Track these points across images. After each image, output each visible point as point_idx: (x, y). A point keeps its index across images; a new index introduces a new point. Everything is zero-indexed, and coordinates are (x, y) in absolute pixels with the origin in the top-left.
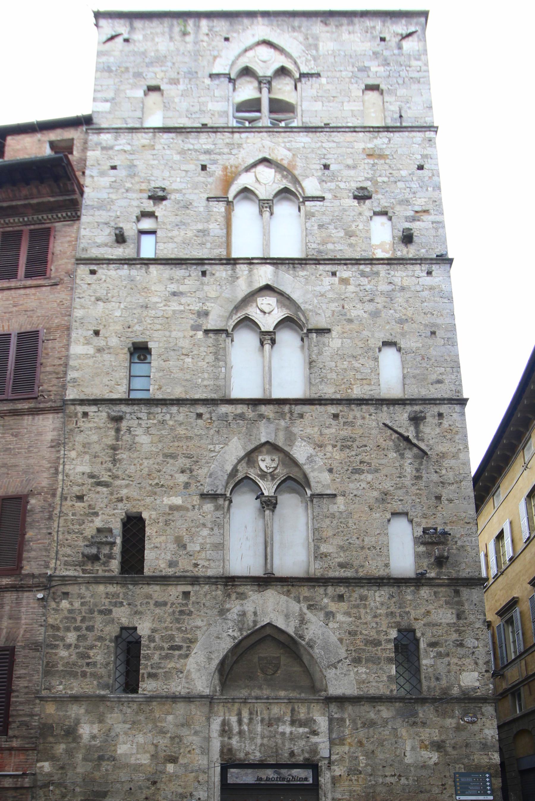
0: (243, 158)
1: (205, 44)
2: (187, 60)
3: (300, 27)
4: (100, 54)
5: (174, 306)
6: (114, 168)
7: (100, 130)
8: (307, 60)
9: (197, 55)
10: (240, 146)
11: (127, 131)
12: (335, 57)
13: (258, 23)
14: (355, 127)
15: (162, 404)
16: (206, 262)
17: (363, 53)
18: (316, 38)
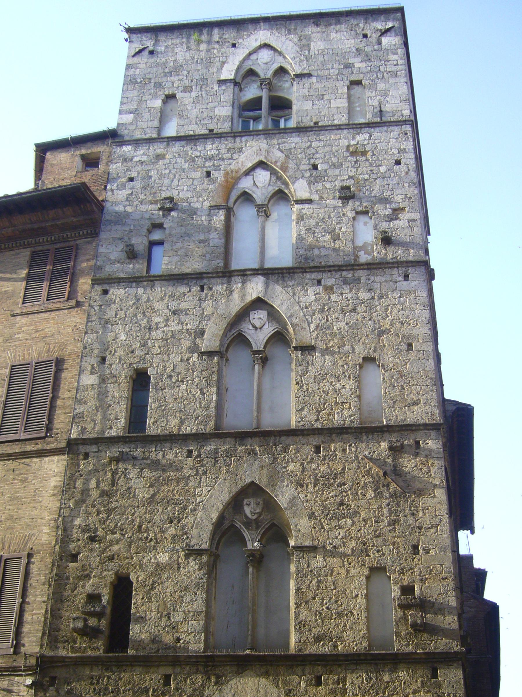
0: (242, 162)
1: (215, 51)
2: (199, 67)
3: (295, 29)
4: (128, 67)
5: (174, 326)
6: (131, 180)
7: (123, 143)
8: (301, 61)
9: (209, 62)
10: (240, 150)
11: (145, 141)
12: (324, 55)
13: (260, 28)
14: (340, 125)
15: (156, 441)
16: (205, 276)
17: (348, 50)
18: (309, 38)
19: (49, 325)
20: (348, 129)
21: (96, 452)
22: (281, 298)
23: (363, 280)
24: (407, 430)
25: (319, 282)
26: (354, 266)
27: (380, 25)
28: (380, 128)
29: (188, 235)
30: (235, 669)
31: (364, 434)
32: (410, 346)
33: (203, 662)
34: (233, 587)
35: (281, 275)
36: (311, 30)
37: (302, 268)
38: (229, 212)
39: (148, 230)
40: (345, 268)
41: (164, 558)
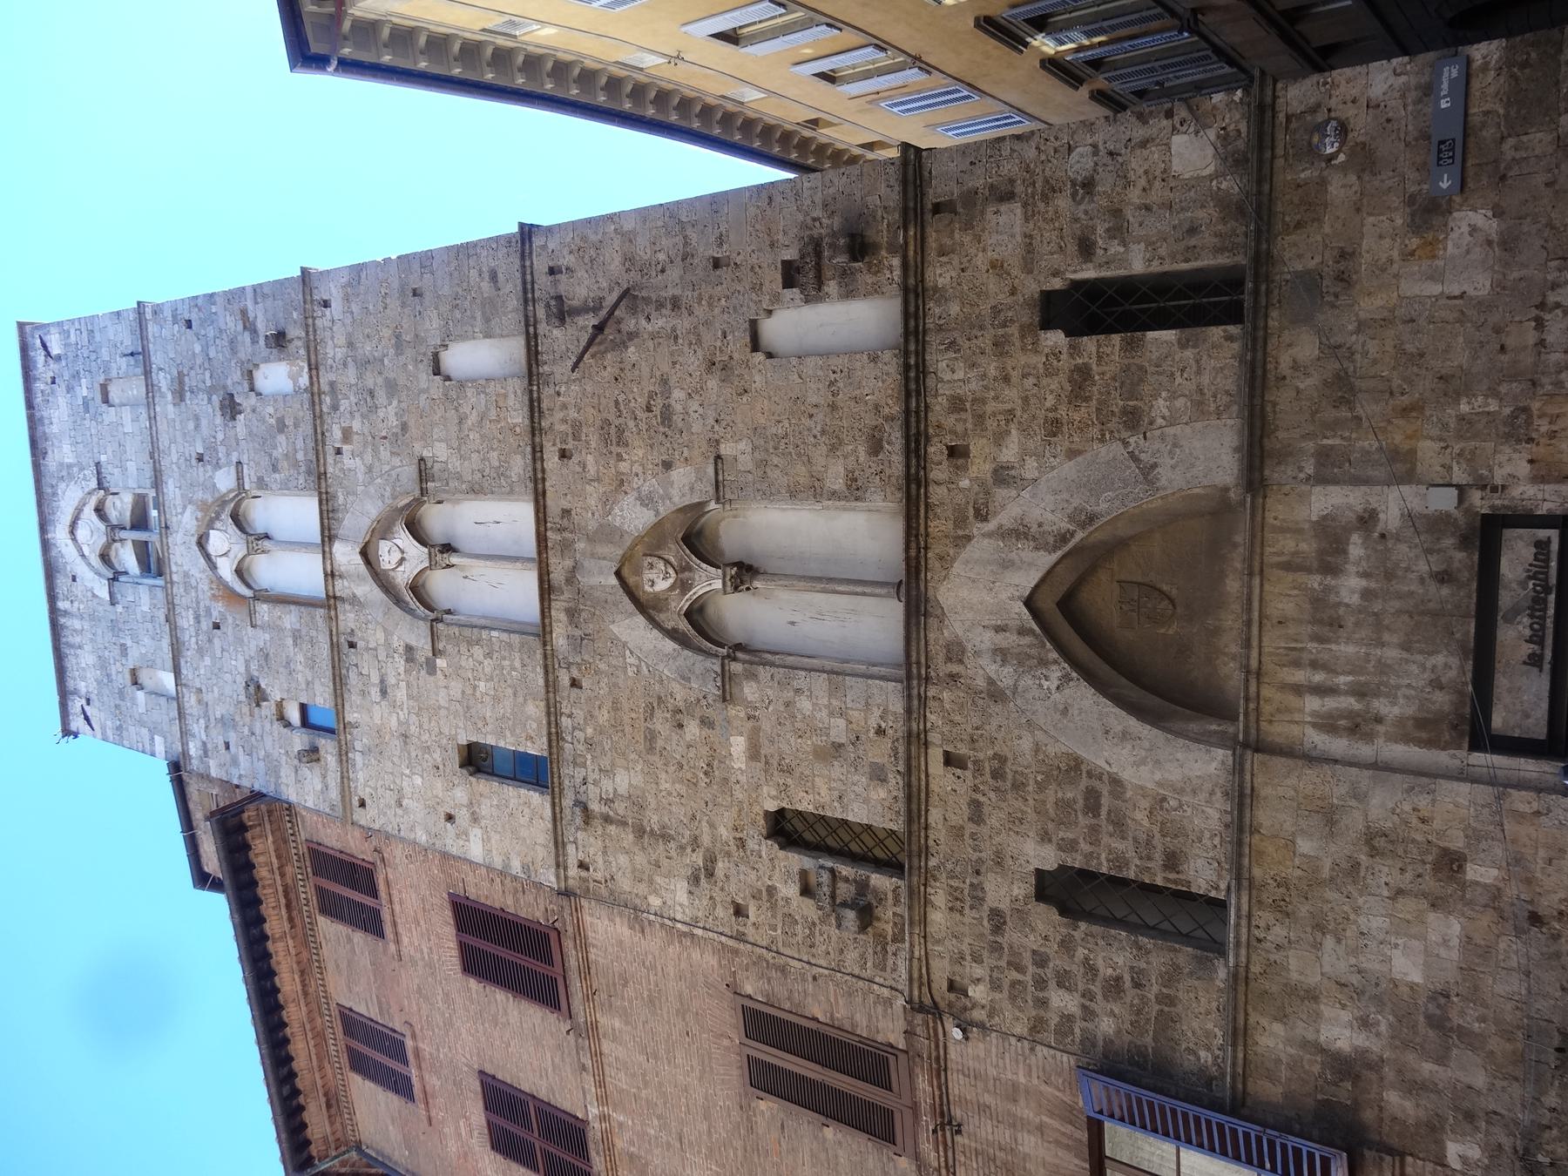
2: (99, 632)
7: (185, 753)
10: (186, 575)
22: (360, 515)
23: (332, 377)
27: (40, 357)
33: (919, 686)
36: (51, 463)
38: (263, 596)
41: (738, 745)
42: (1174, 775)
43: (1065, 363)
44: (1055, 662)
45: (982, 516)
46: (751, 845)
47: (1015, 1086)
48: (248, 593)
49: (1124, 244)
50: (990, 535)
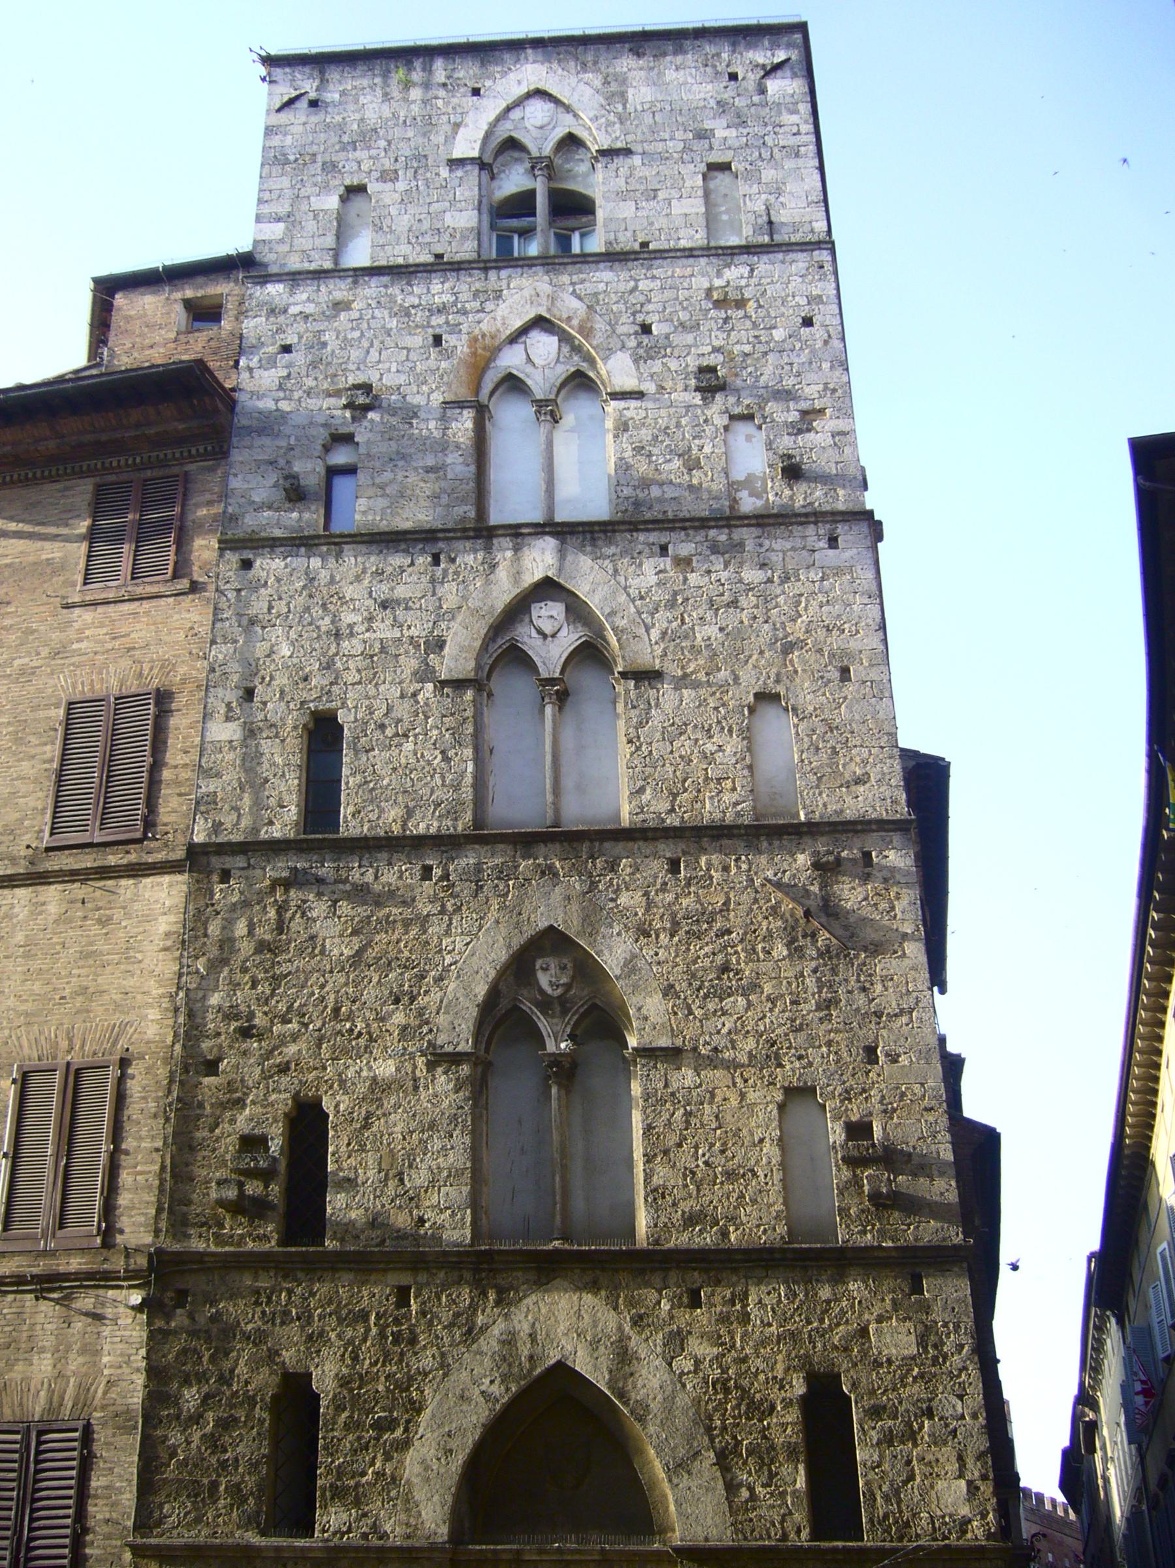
0: (503, 318)
1: (440, 103)
3: (595, 63)
5: (384, 631)
7: (265, 279)
8: (609, 124)
9: (428, 124)
10: (498, 295)
11: (310, 276)
12: (654, 113)
13: (526, 59)
14: (691, 249)
15: (361, 848)
16: (440, 535)
17: (702, 104)
18: (623, 81)
19: (138, 626)
20: (708, 256)
21: (243, 869)
22: (589, 577)
24: (847, 831)
25: (664, 550)
26: (730, 519)
28: (771, 256)
29: (403, 457)
30: (532, 1276)
31: (762, 838)
32: (845, 672)
34: (520, 1122)
35: (588, 536)
36: (626, 64)
37: (630, 523)
38: (482, 413)
39: (324, 446)
40: (713, 524)
42: (419, 1495)
43: (775, 1395)
44: (507, 1389)
45: (637, 1321)
46: (285, 1080)
47: (98, 1353)
48: (484, 397)
49: (879, 1443)
50: (620, 1328)
